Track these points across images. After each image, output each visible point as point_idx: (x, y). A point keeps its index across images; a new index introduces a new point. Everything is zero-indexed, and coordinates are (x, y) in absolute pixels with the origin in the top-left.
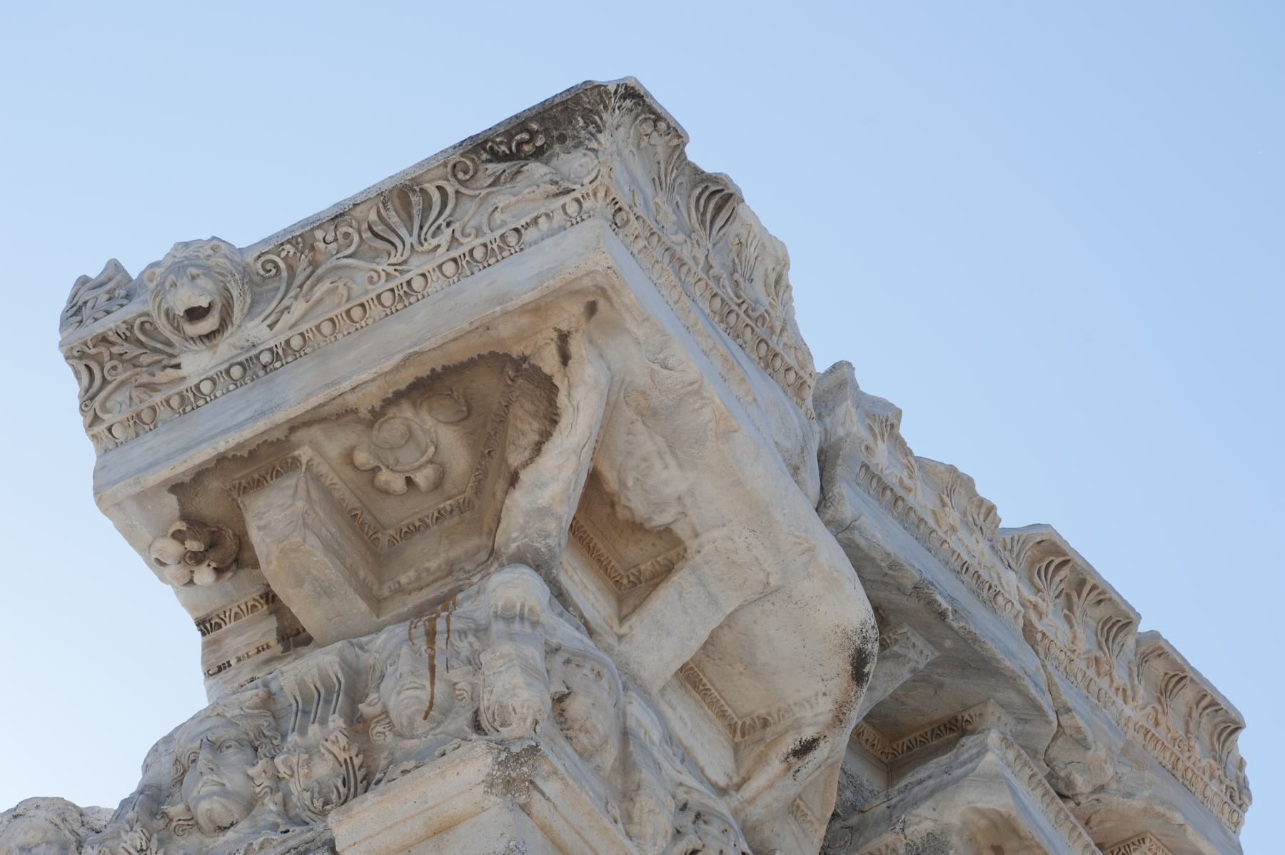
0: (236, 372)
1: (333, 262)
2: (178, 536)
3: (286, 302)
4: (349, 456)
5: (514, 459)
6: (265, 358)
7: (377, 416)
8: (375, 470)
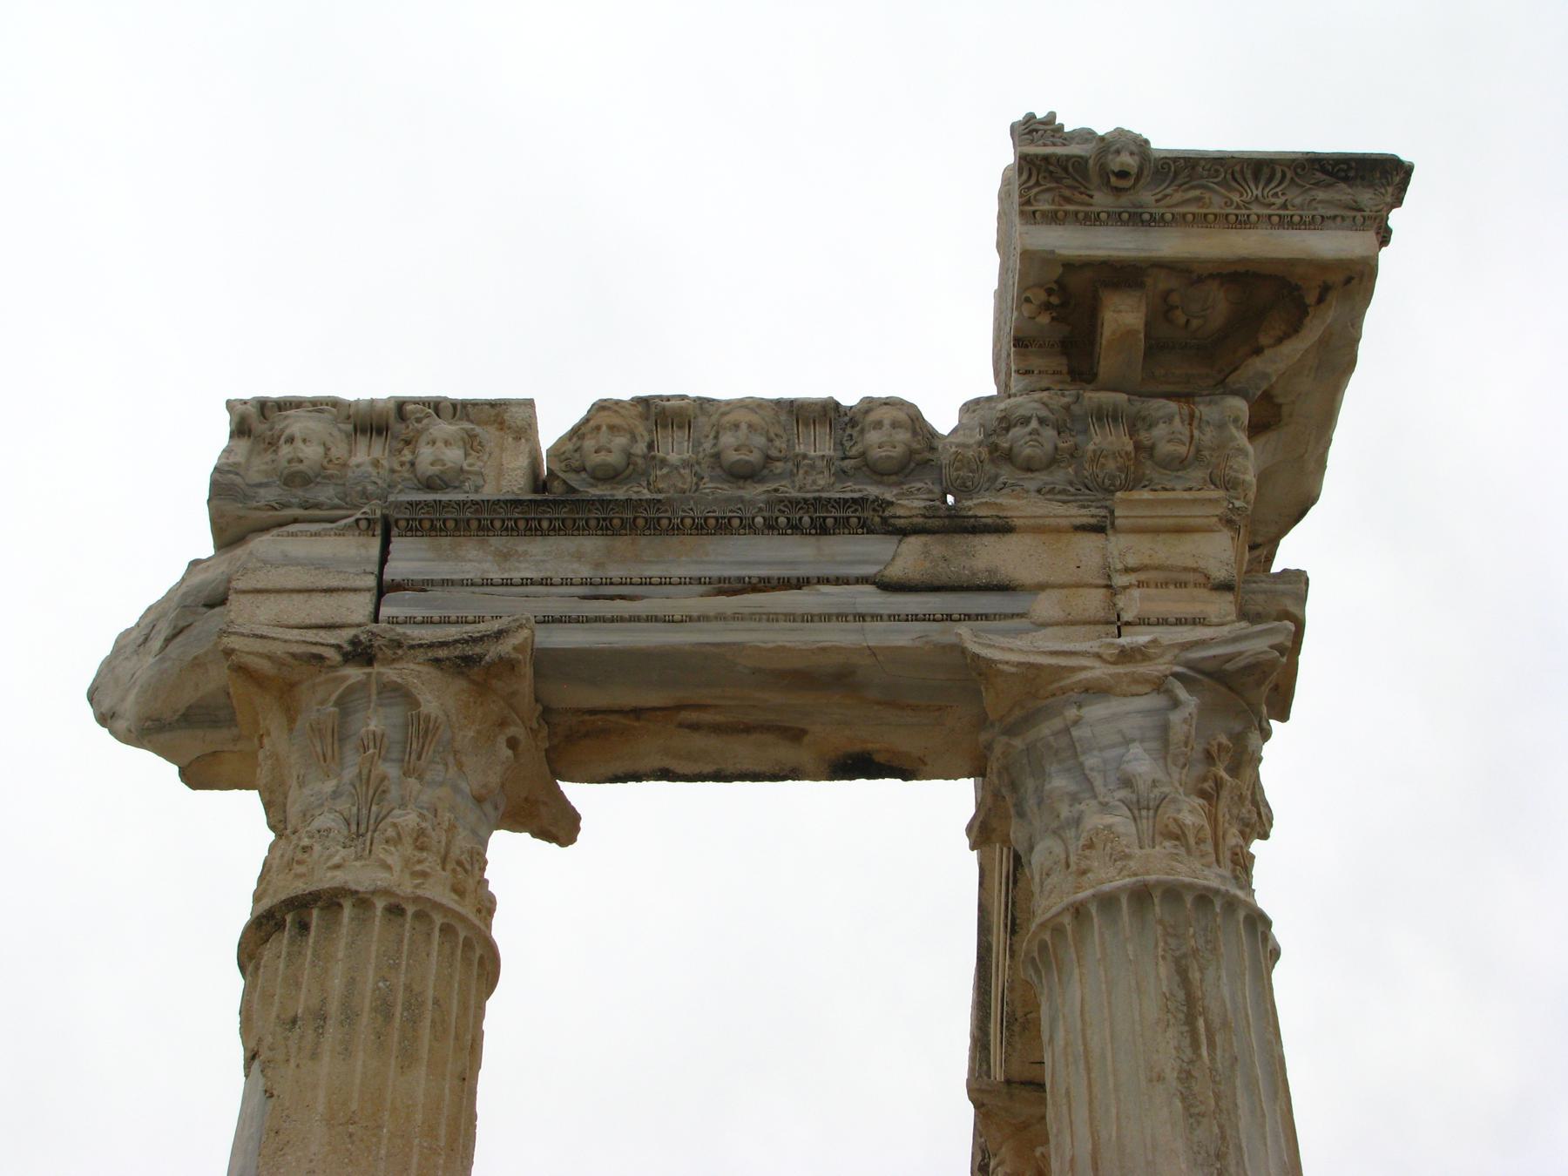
0: (1125, 216)
1: (1204, 182)
2: (1050, 292)
3: (1169, 191)
4: (1166, 295)
5: (1264, 340)
6: (1146, 217)
7: (1200, 280)
8: (1172, 308)
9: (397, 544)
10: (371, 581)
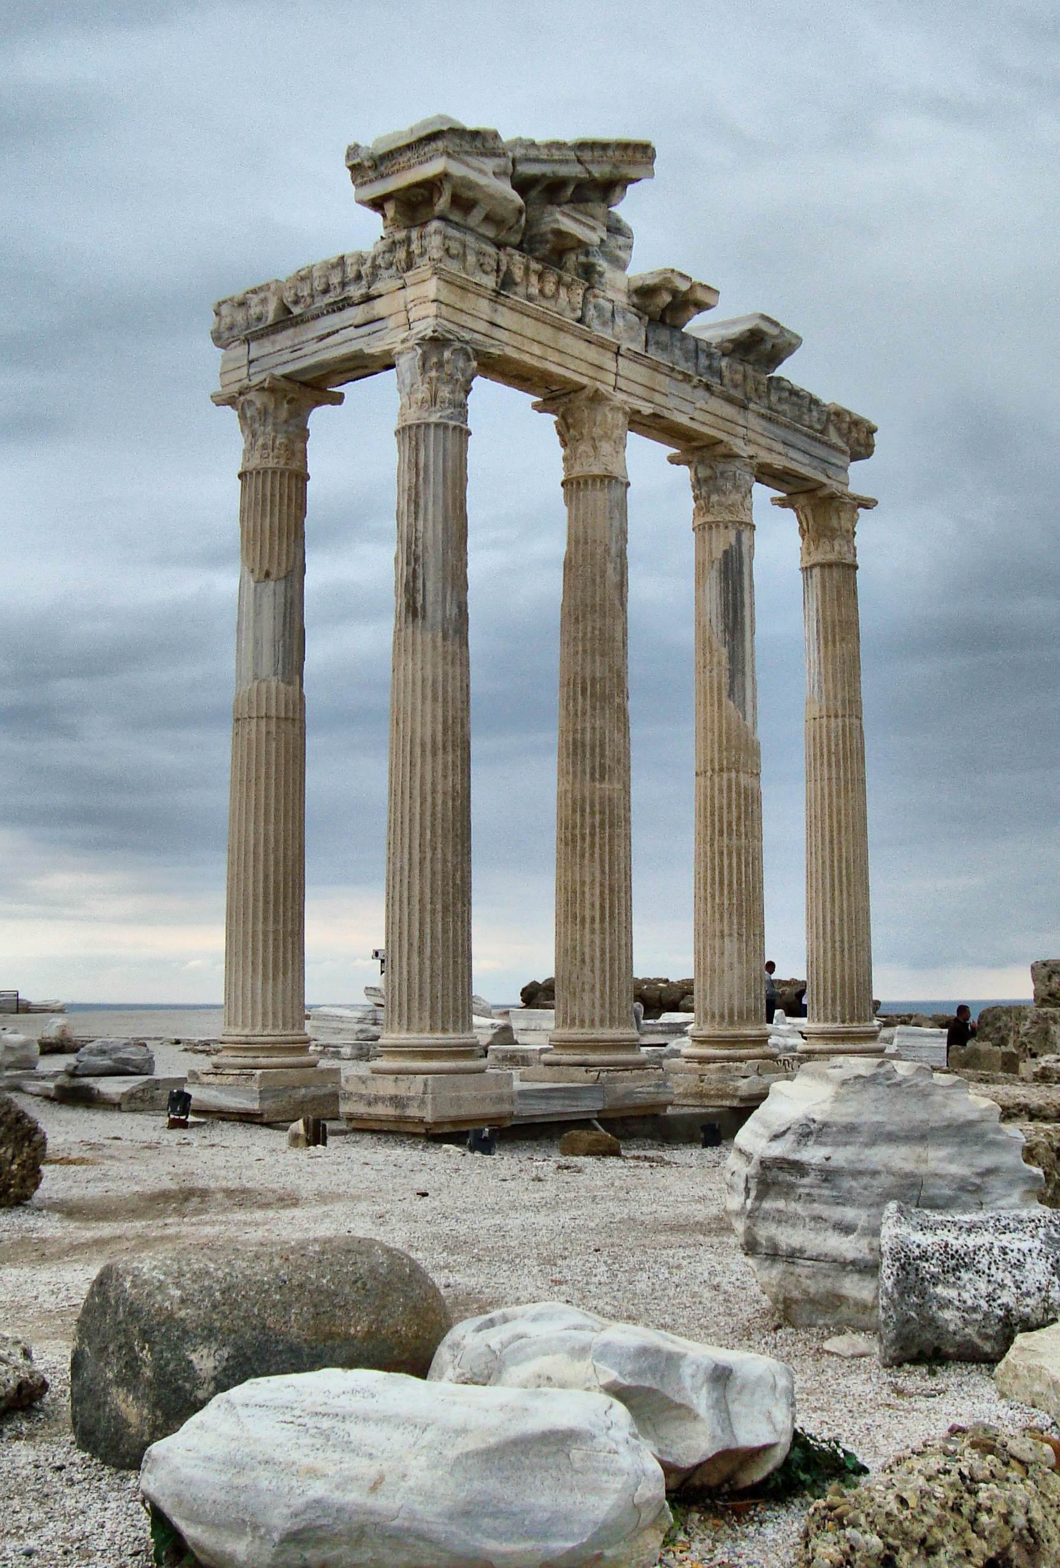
9: (252, 345)
10: (246, 362)
